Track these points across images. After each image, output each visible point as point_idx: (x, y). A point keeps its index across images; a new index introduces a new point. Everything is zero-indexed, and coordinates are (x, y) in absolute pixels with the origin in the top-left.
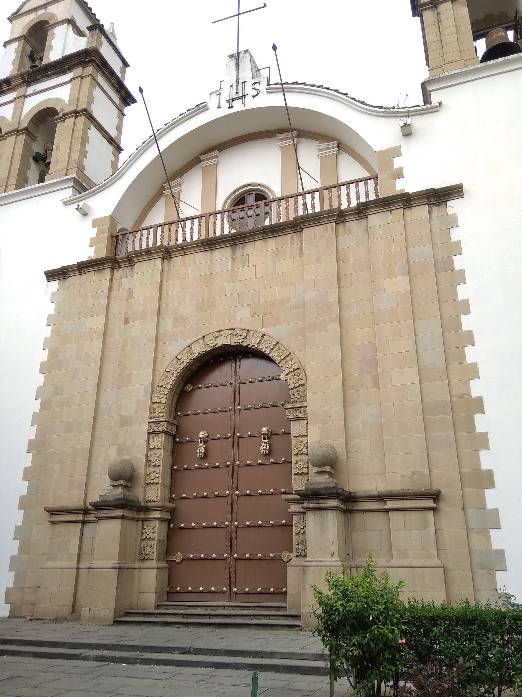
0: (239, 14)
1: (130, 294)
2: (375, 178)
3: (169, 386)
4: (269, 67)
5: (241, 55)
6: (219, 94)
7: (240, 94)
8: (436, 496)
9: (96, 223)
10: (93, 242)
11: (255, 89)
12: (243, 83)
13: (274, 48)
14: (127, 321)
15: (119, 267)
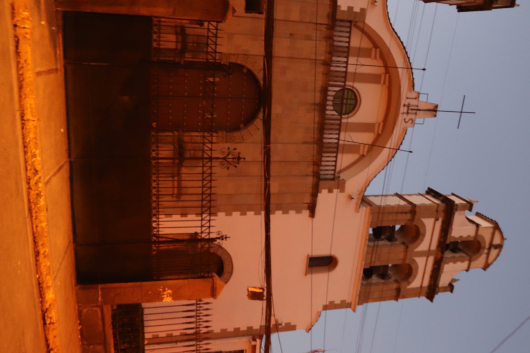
0: (461, 112)
1: (308, 38)
2: (333, 179)
3: (246, 65)
4: (423, 124)
5: (434, 113)
6: (416, 98)
7: (410, 111)
8: (179, 195)
9: (363, 11)
10: (350, 9)
11: (410, 120)
12: (416, 114)
13: (411, 152)
14: (291, 35)
15: (327, 28)
